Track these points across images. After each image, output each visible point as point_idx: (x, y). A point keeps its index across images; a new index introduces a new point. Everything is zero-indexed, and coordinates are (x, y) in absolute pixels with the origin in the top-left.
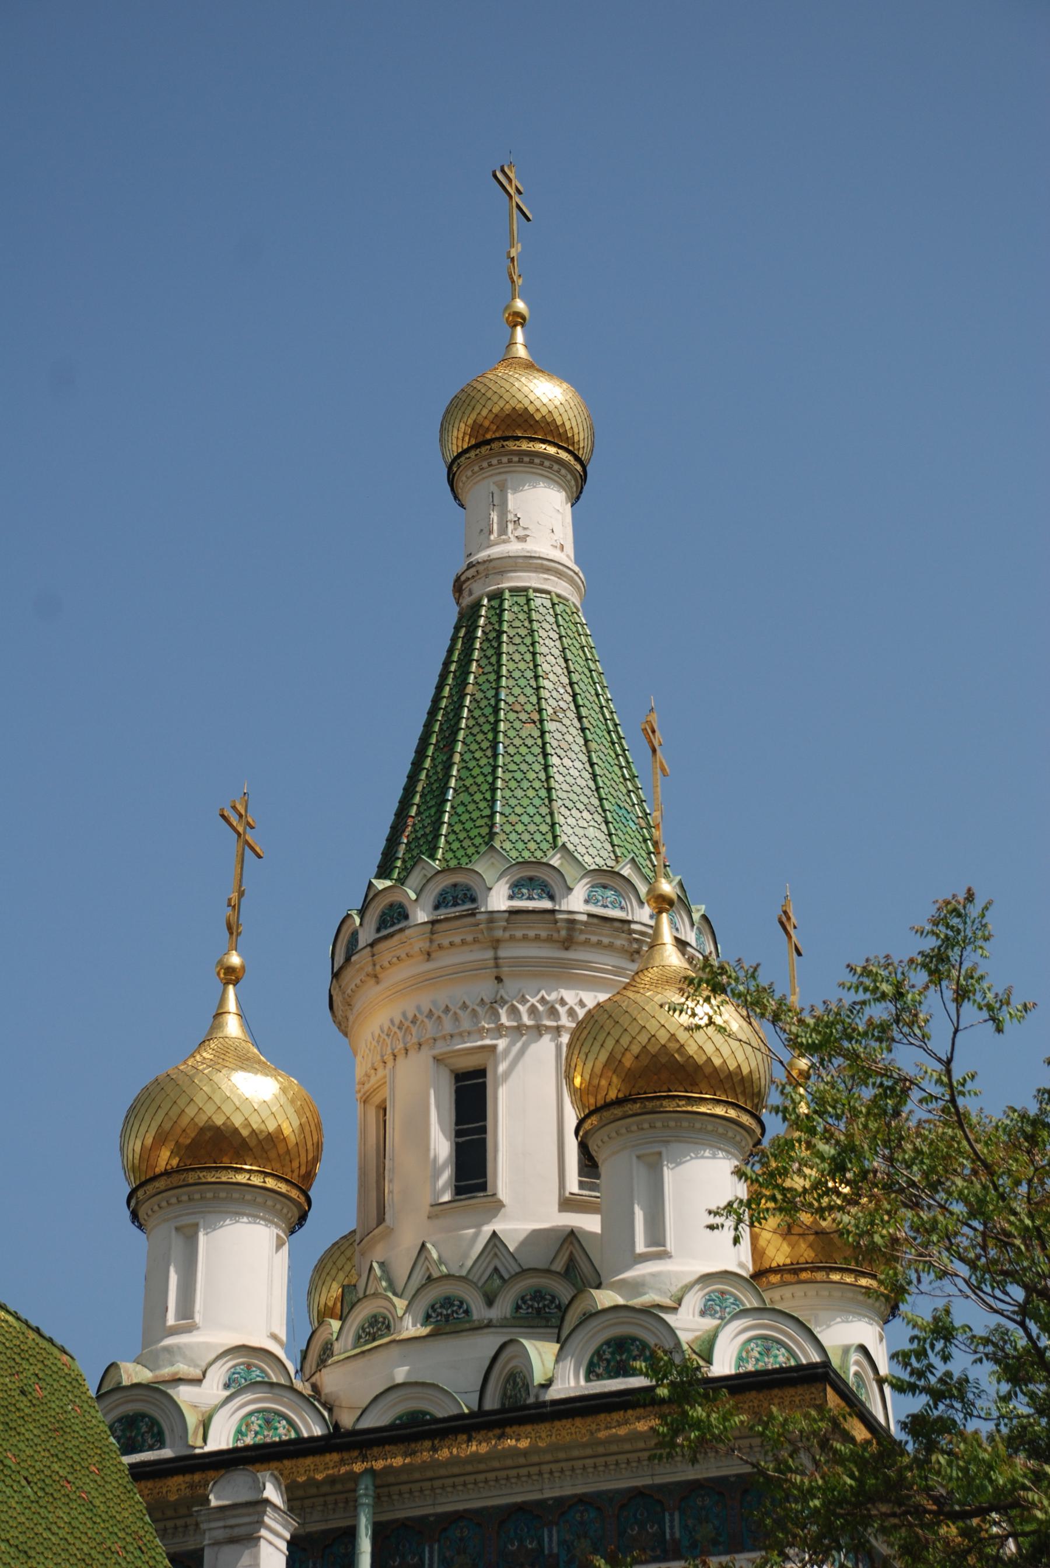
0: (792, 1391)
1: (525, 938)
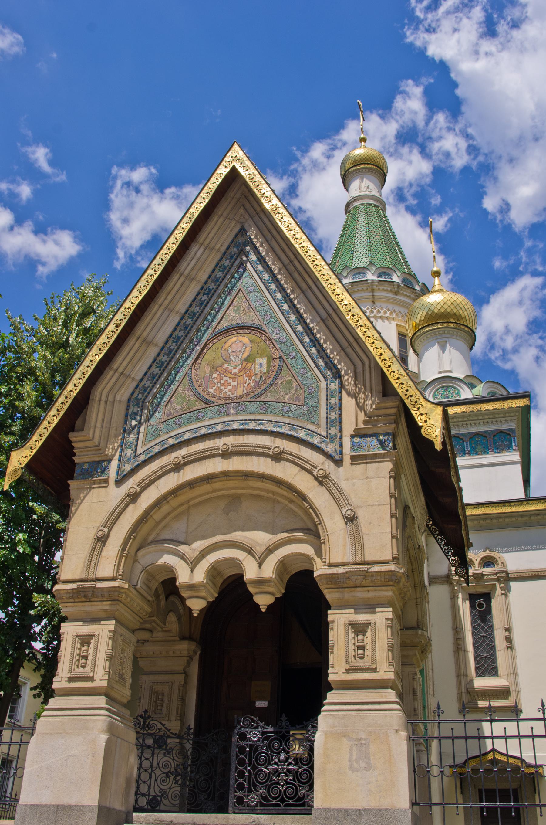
0: (516, 401)
1: (383, 290)
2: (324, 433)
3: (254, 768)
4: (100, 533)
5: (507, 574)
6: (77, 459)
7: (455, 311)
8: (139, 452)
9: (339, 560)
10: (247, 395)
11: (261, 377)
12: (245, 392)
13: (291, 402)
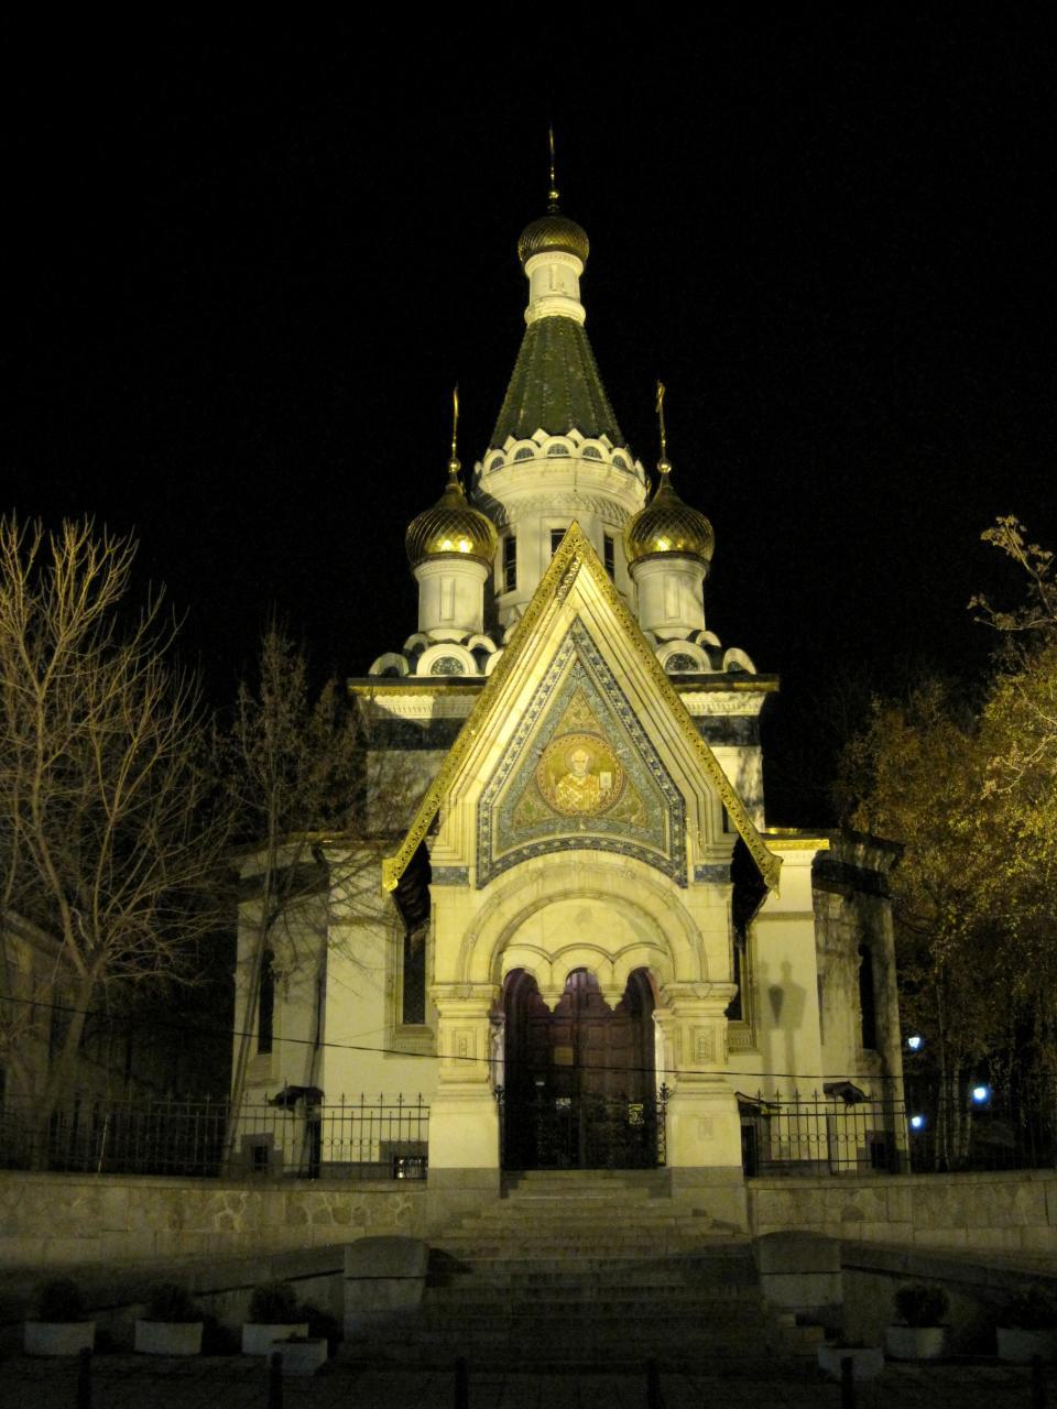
10: (594, 810)
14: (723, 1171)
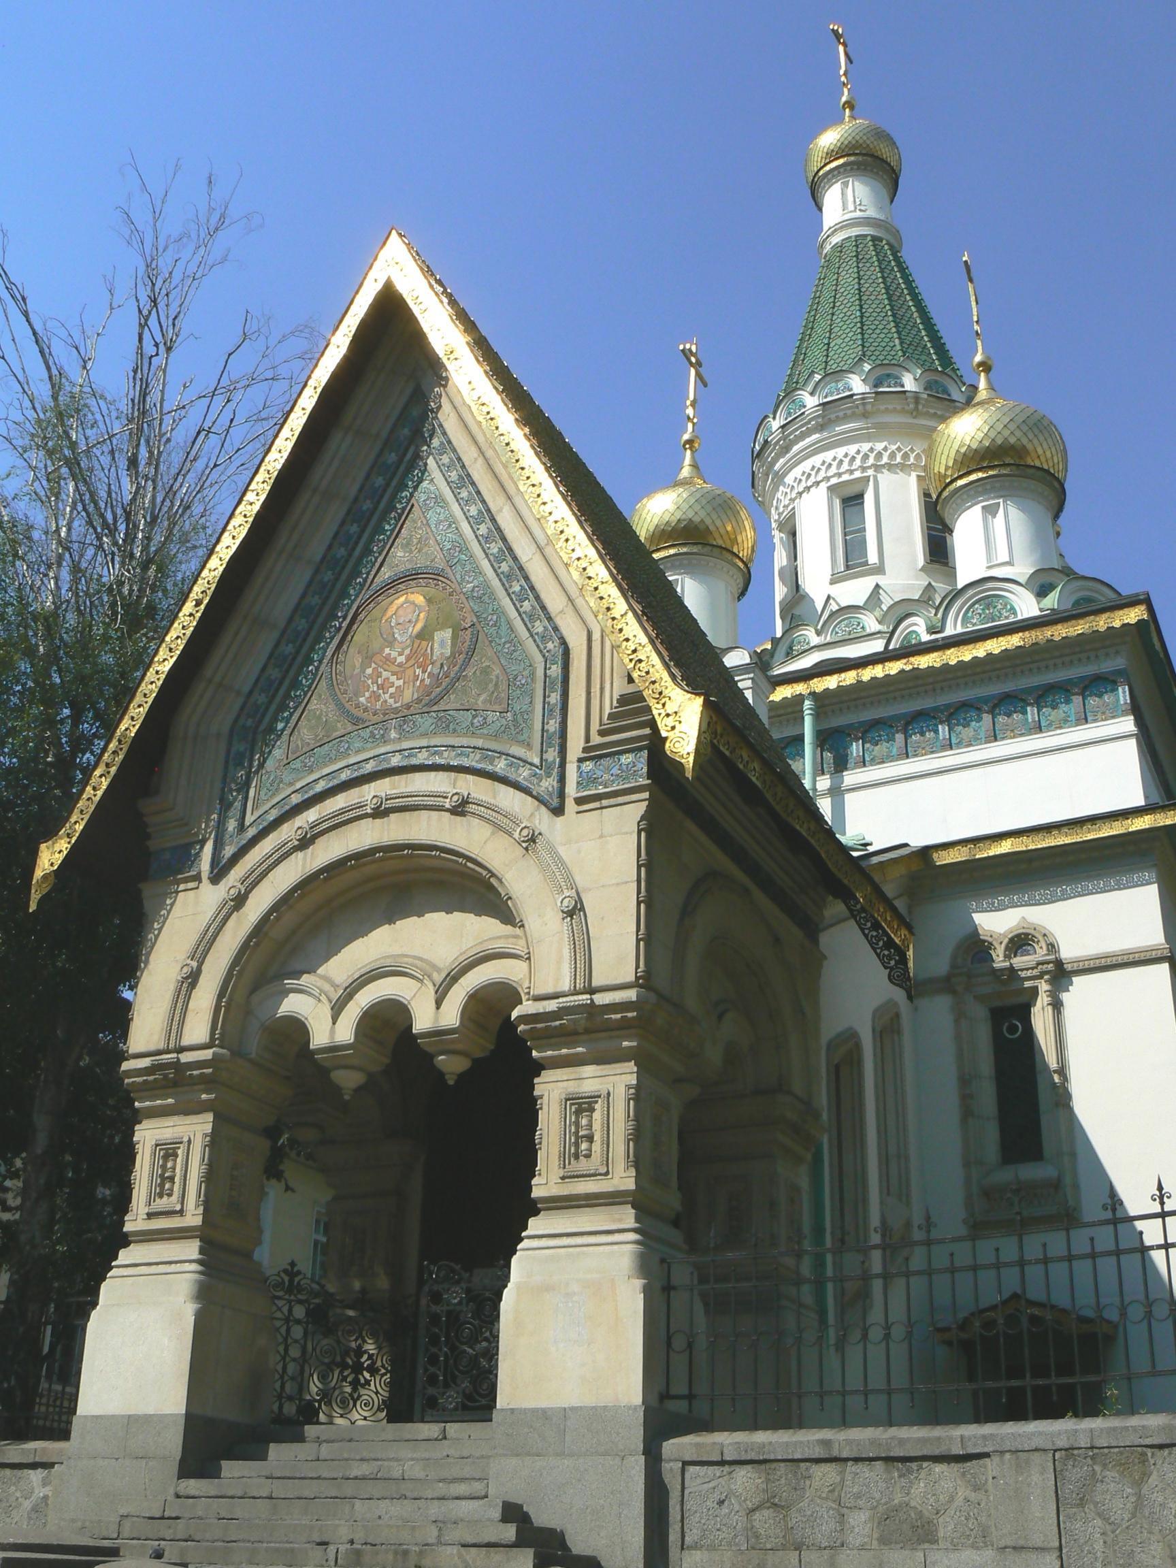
0: (1121, 612)
2: (536, 761)
3: (453, 1348)
4: (185, 970)
5: (1059, 963)
6: (153, 845)
7: (1012, 440)
8: (247, 823)
9: (550, 989)
10: (419, 701)
11: (442, 665)
12: (416, 696)
13: (488, 707)
14: (596, 1417)
